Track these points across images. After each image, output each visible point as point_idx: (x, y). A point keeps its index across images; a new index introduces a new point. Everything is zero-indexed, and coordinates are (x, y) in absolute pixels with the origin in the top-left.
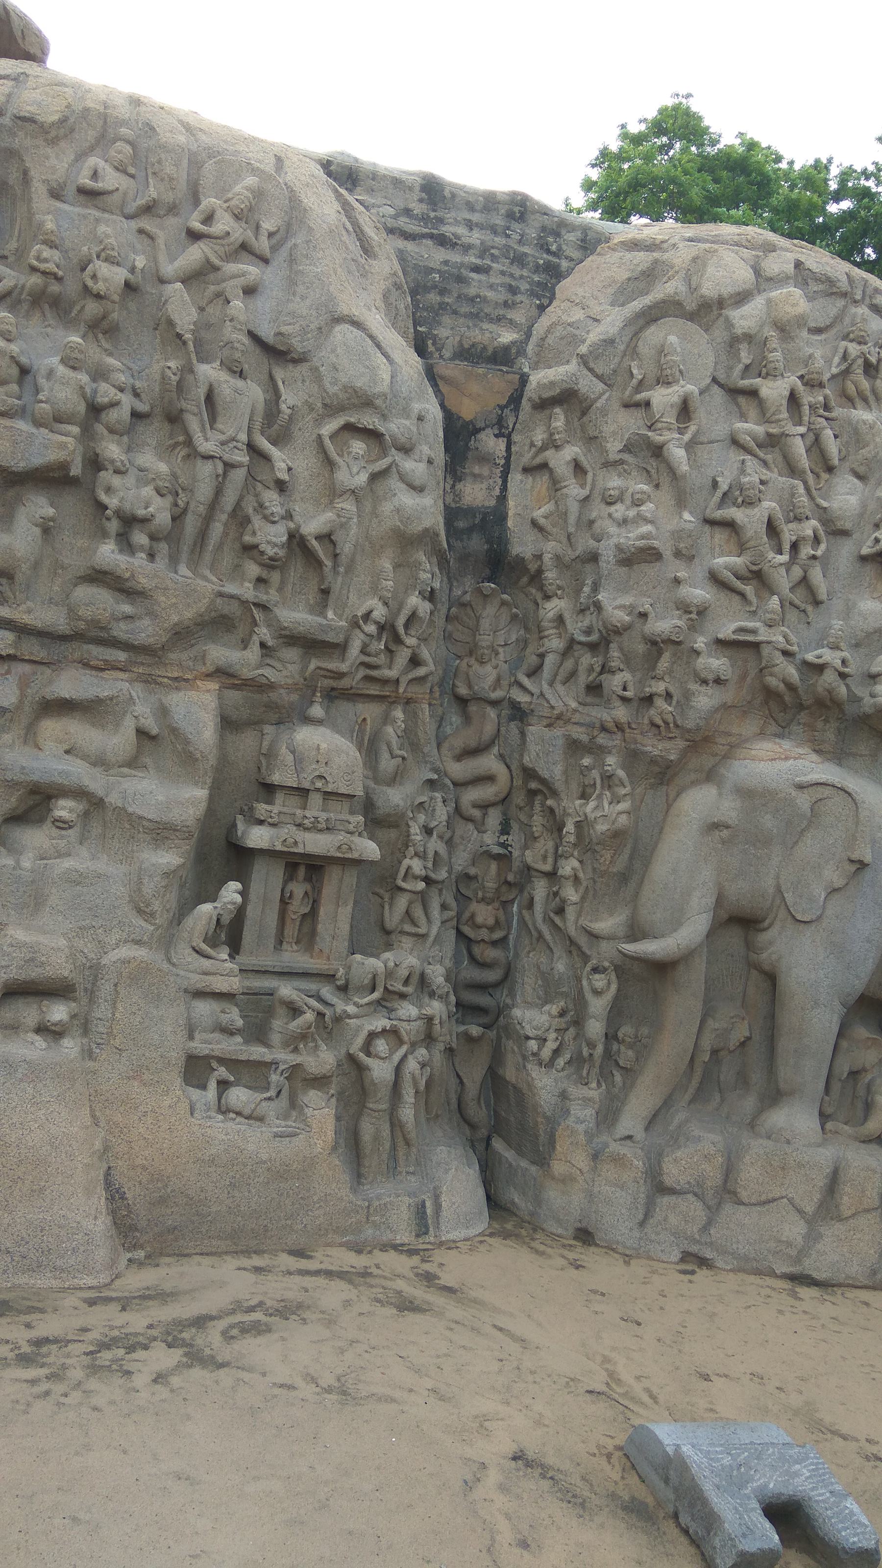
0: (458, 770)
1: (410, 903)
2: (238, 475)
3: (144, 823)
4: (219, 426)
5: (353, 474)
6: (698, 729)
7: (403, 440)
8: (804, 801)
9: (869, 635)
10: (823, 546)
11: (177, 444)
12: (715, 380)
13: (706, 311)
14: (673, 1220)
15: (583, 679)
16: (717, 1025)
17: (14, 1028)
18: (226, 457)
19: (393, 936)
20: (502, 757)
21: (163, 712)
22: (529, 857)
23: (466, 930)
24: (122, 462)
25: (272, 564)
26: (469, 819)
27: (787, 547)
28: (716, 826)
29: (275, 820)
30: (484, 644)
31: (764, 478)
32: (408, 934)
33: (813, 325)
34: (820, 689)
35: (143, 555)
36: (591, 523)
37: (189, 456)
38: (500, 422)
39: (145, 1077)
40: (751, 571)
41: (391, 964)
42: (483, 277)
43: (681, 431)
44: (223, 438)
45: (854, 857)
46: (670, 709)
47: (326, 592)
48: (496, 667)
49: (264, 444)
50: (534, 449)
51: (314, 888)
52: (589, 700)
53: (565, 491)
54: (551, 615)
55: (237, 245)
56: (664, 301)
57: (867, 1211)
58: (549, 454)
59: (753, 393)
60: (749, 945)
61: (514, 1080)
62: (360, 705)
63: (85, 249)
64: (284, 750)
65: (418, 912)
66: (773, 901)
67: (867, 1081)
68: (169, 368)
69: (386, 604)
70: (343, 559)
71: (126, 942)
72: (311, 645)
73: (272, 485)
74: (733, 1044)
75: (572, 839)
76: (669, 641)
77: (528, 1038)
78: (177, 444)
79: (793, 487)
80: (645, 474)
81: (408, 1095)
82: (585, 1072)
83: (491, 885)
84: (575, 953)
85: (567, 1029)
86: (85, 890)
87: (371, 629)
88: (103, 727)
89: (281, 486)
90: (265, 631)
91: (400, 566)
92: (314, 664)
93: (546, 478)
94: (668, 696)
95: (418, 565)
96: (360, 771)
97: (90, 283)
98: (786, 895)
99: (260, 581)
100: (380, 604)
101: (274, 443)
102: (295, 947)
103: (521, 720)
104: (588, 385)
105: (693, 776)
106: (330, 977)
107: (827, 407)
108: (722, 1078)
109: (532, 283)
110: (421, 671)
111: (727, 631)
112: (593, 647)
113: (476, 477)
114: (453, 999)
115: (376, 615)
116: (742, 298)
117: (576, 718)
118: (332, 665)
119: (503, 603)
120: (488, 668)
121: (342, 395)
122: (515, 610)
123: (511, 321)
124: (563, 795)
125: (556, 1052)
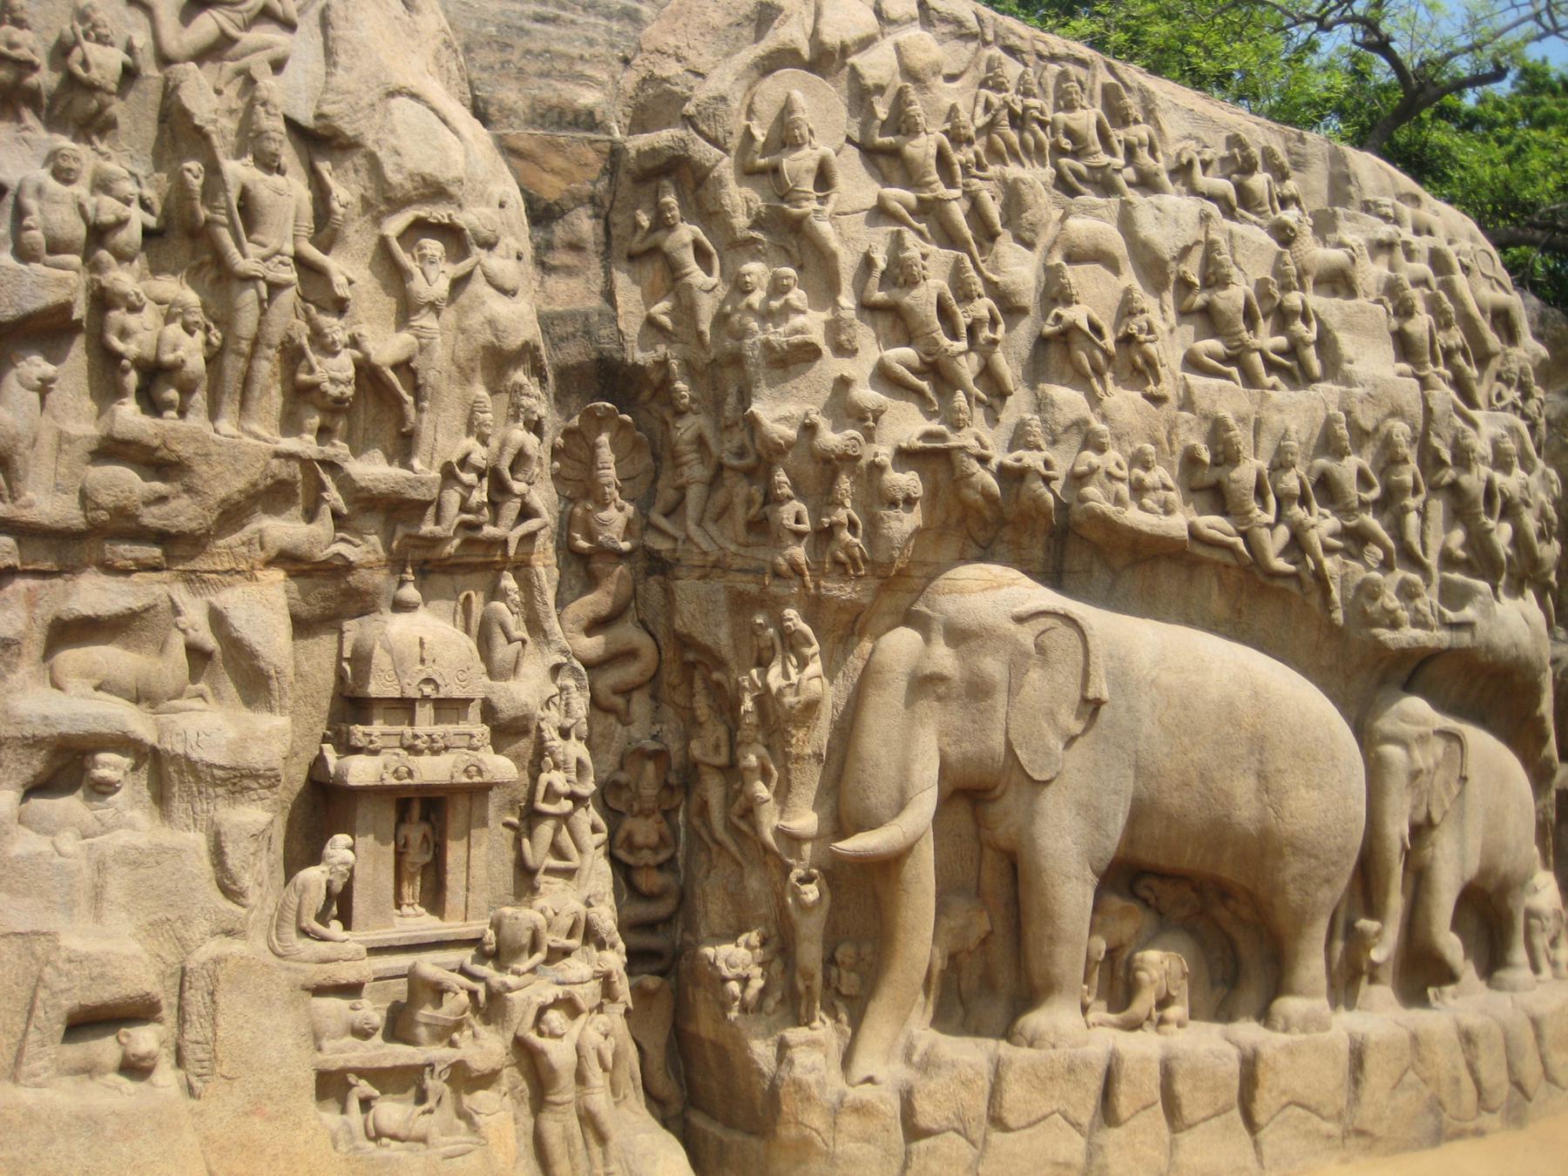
1: (557, 831)
2: (288, 297)
3: (216, 772)
4: (255, 236)
5: (432, 280)
7: (485, 233)
8: (1026, 635)
9: (1067, 429)
10: (1002, 327)
11: (202, 265)
12: (849, 140)
13: (824, 60)
14: (934, 1166)
15: (740, 515)
16: (952, 923)
17: (89, 1070)
18: (271, 276)
19: (541, 878)
20: (643, 624)
21: (217, 619)
22: (696, 749)
23: (622, 854)
24: (137, 294)
25: (336, 407)
29: (379, 744)
33: (946, 71)
34: (1024, 498)
35: (173, 414)
37: (219, 279)
39: (268, 1109)
41: (550, 913)
42: (550, 29)
43: (823, 200)
44: (264, 252)
45: (1091, 694)
49: (313, 253)
50: (640, 234)
51: (433, 828)
52: (752, 539)
53: (688, 279)
54: (688, 436)
55: (256, 11)
56: (779, 51)
57: (1145, 1108)
58: (659, 235)
59: (895, 153)
60: (978, 821)
61: (712, 1036)
62: (460, 579)
63: (67, 27)
64: (378, 652)
67: (1125, 957)
68: (189, 170)
71: (214, 934)
72: (394, 510)
73: (329, 305)
75: (751, 719)
77: (725, 980)
78: (202, 265)
79: (958, 261)
84: (771, 864)
85: (771, 961)
86: (151, 871)
87: (469, 477)
88: (138, 648)
89: (340, 307)
90: (337, 495)
92: (401, 531)
93: (658, 265)
94: (852, 526)
95: (519, 389)
97: (79, 71)
98: (1018, 752)
99: (324, 433)
101: (326, 251)
103: (663, 572)
104: (702, 150)
105: (888, 620)
107: (980, 166)
108: (963, 987)
109: (609, 31)
112: (749, 474)
113: (570, 271)
114: (621, 946)
116: (866, 43)
117: (738, 563)
119: (624, 424)
121: (409, 185)
122: (639, 434)
123: (590, 78)
124: (733, 664)
125: (763, 992)
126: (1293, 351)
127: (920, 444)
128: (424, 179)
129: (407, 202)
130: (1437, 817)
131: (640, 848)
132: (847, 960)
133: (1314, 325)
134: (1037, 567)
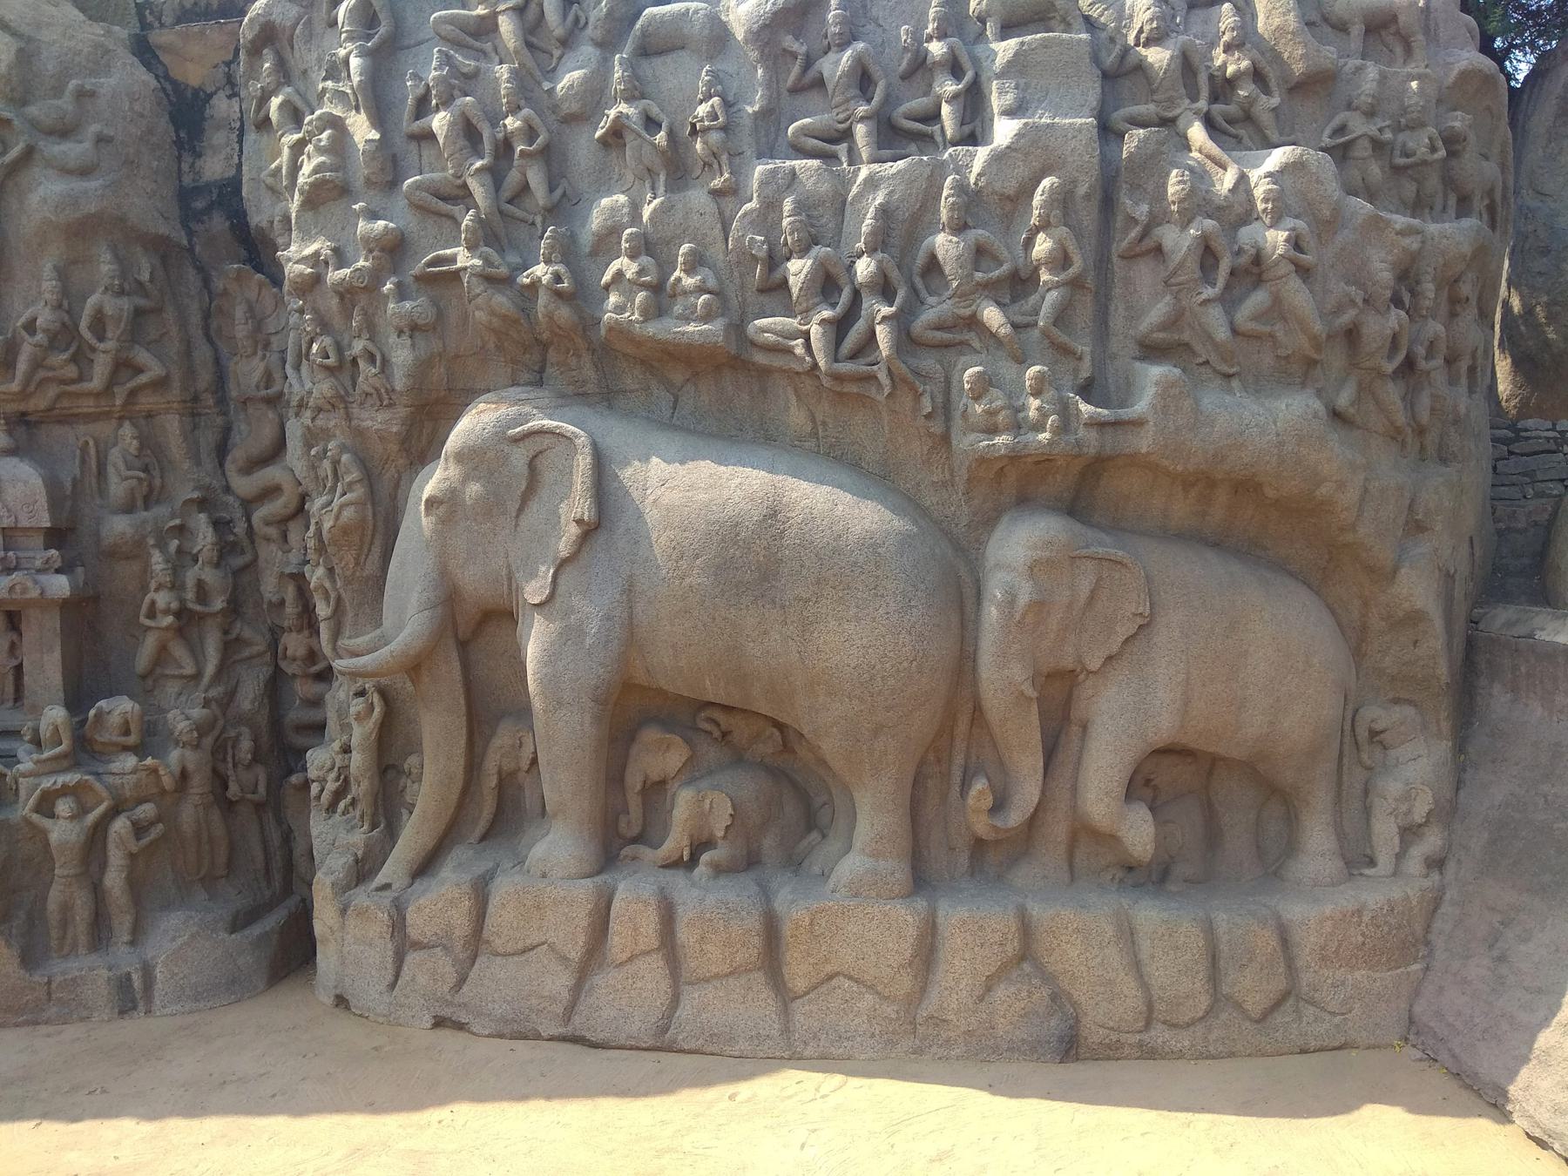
0: (244, 485)
6: (410, 389)
8: (519, 458)
14: (422, 980)
19: (150, 682)
23: (283, 665)
26: (268, 539)
27: (487, 146)
28: (432, 503)
31: (465, 70)
32: (174, 677)
38: (230, 81)
40: (459, 187)
43: (369, 37)
62: (82, 428)
65: (179, 651)
66: (510, 585)
74: (525, 764)
75: (311, 544)
81: (116, 858)
82: (358, 813)
83: (291, 609)
94: (371, 358)
96: (42, 500)
102: (10, 704)
106: (14, 734)
110: (143, 379)
111: (420, 265)
114: (246, 744)
120: (256, 361)
124: (314, 494)
125: (339, 795)
126: (935, 116)
130: (1094, 663)
131: (294, 660)
132: (414, 771)
133: (969, 76)
134: (590, 388)
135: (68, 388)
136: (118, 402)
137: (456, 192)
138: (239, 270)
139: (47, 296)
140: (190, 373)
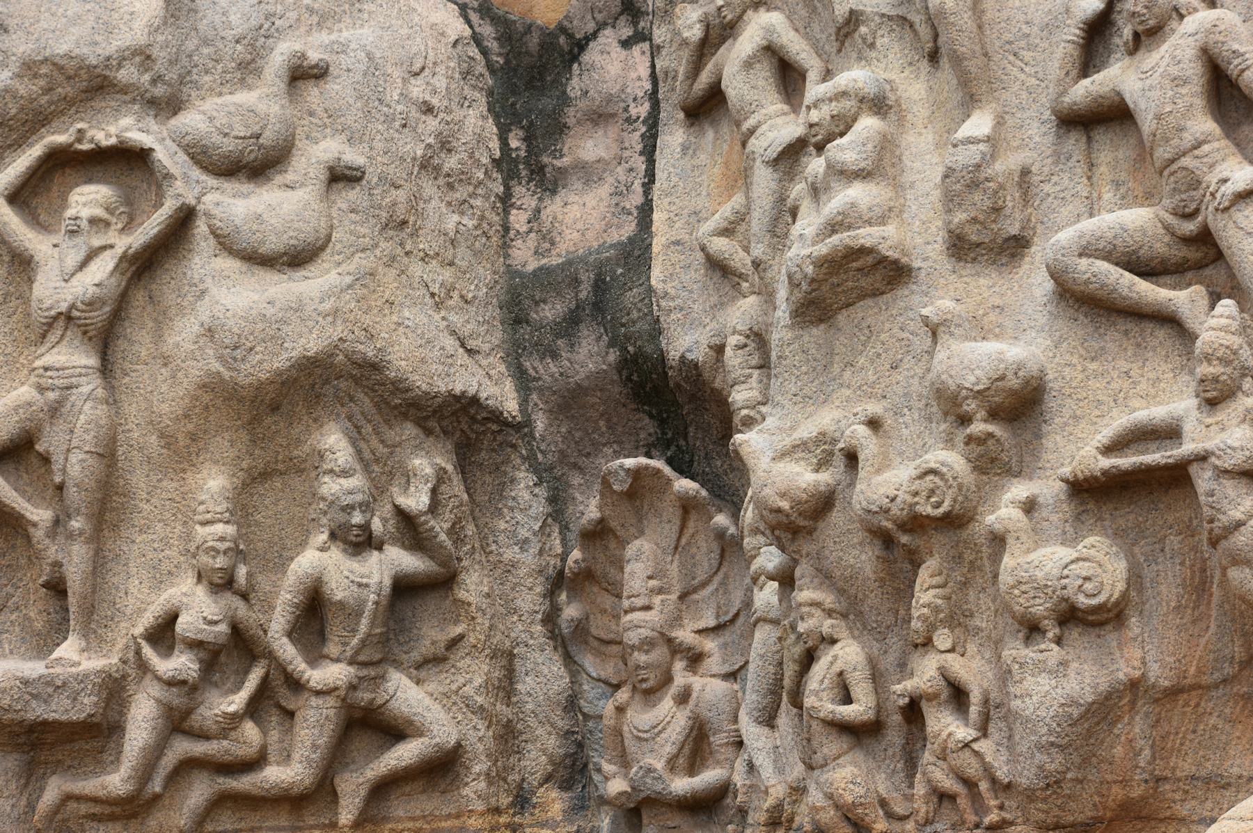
6: (1054, 784)
7: (229, 145)
30: (632, 637)
36: (794, 212)
40: (1187, 240)
46: (962, 732)
47: (57, 588)
48: (683, 698)
69: (223, 584)
70: (72, 492)
76: (915, 523)
80: (908, 35)
91: (265, 475)
92: (52, 791)
100: (201, 592)
110: (405, 754)
113: (589, 173)
115: (182, 624)
118: (90, 786)
119: (687, 506)
120: (667, 704)
127: (1106, 463)
128: (60, 68)
129: (37, 120)
135: (244, 783)
136: (346, 816)
137: (1180, 253)
138: (637, 473)
139: (205, 559)
140: (509, 737)
